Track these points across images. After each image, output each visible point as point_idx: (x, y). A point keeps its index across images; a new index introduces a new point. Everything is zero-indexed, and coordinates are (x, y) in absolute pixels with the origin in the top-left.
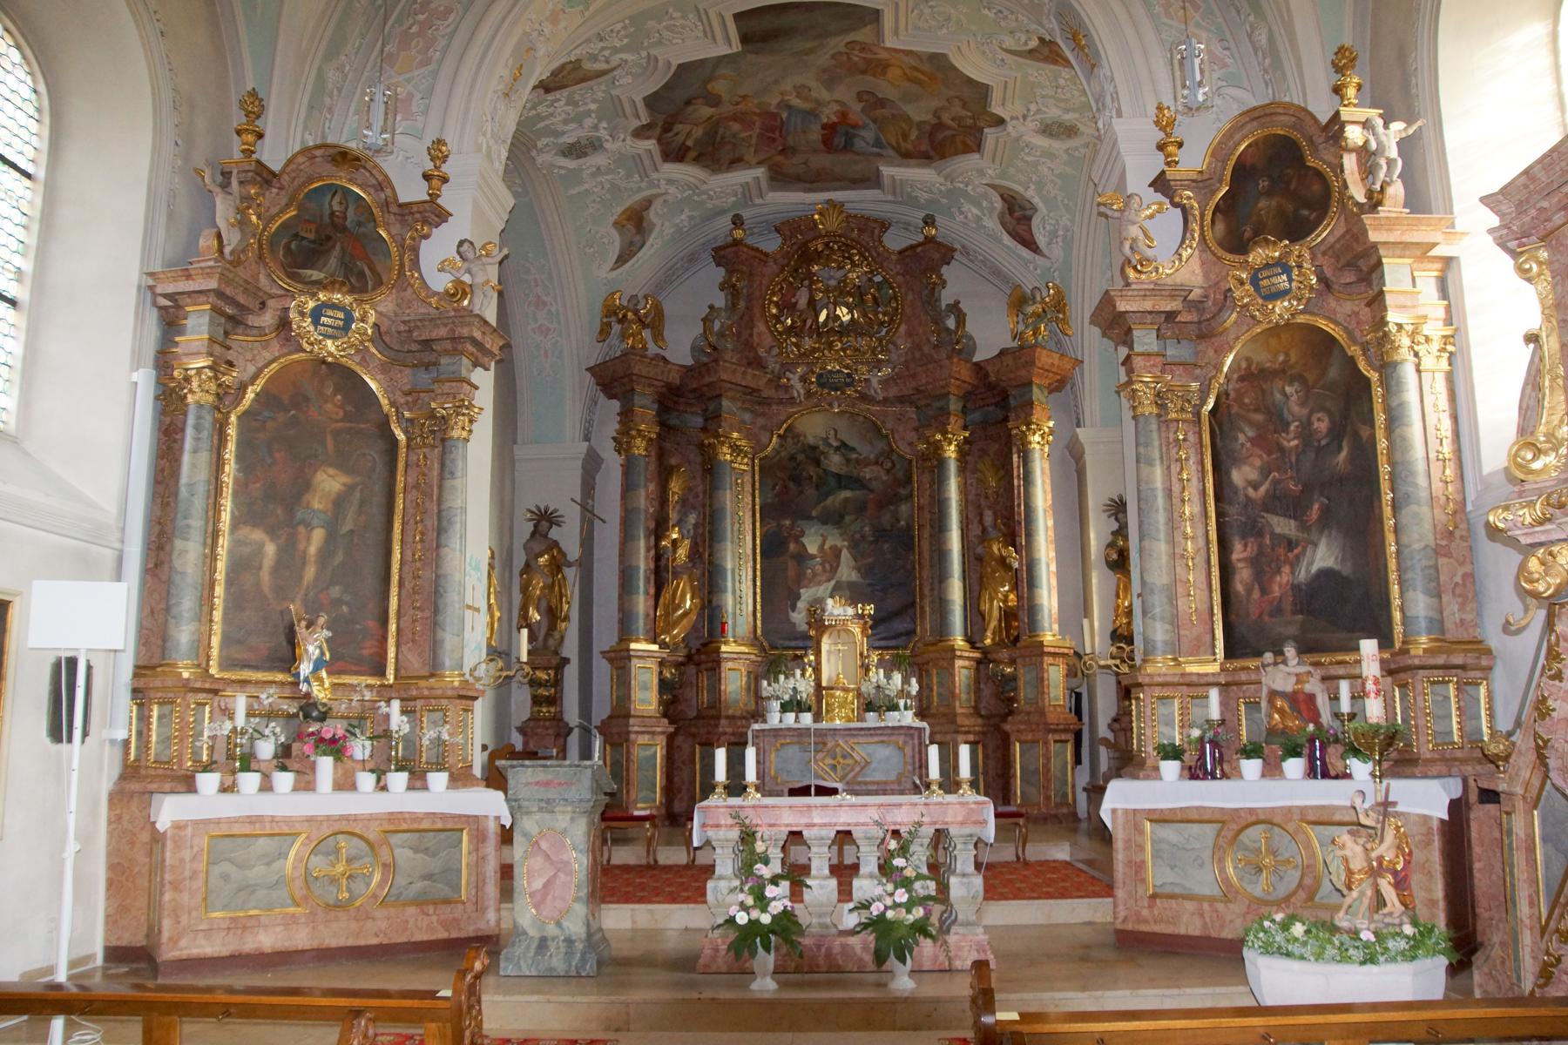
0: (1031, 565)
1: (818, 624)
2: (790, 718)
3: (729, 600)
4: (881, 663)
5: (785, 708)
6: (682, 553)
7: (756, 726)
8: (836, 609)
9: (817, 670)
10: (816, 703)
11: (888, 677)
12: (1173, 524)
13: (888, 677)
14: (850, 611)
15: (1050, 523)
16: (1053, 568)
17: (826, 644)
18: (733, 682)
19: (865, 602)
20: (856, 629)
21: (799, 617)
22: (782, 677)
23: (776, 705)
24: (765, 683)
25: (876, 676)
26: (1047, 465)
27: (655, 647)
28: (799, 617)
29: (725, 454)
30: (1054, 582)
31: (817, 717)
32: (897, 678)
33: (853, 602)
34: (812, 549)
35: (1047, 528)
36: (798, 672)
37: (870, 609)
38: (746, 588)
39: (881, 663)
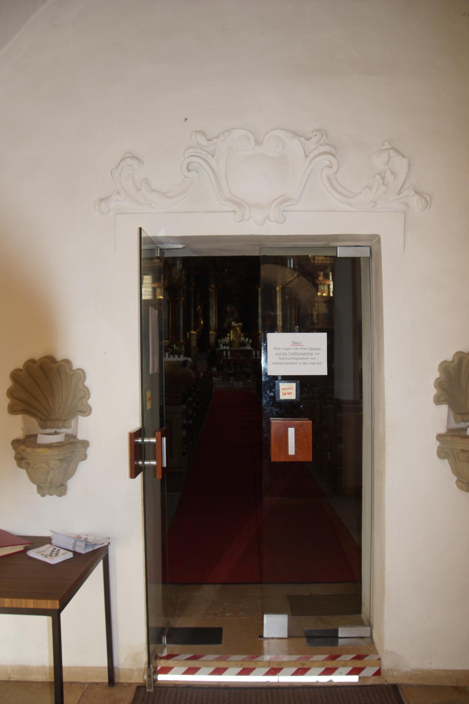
0: (276, 316)
1: (230, 327)
2: (225, 347)
3: (211, 322)
4: (243, 336)
5: (224, 345)
6: (201, 312)
7: (218, 349)
8: (233, 324)
9: (230, 337)
10: (231, 344)
11: (245, 339)
12: (291, 319)
13: (245, 339)
14: (237, 325)
15: (280, 306)
16: (281, 316)
17: (231, 332)
18: (212, 340)
19: (240, 323)
20: (238, 329)
21: (225, 325)
22: (222, 339)
23: (221, 345)
24: (219, 340)
25: (243, 339)
26: (280, 293)
27: (195, 332)
28: (225, 325)
29: (210, 289)
30: (281, 319)
31: (230, 347)
32: (247, 339)
33: (237, 322)
34: (228, 310)
35: (279, 307)
36: (226, 338)
37: (241, 324)
38: (214, 319)
39: (243, 336)
